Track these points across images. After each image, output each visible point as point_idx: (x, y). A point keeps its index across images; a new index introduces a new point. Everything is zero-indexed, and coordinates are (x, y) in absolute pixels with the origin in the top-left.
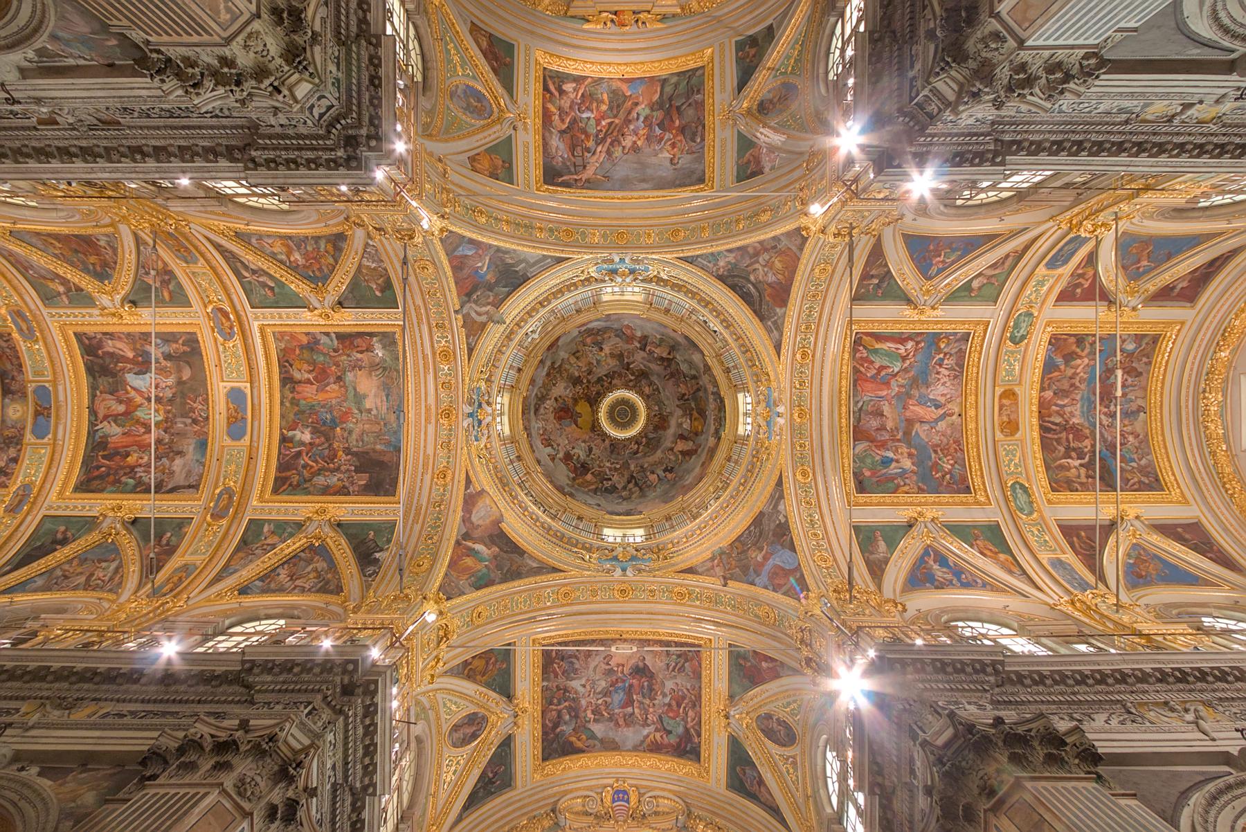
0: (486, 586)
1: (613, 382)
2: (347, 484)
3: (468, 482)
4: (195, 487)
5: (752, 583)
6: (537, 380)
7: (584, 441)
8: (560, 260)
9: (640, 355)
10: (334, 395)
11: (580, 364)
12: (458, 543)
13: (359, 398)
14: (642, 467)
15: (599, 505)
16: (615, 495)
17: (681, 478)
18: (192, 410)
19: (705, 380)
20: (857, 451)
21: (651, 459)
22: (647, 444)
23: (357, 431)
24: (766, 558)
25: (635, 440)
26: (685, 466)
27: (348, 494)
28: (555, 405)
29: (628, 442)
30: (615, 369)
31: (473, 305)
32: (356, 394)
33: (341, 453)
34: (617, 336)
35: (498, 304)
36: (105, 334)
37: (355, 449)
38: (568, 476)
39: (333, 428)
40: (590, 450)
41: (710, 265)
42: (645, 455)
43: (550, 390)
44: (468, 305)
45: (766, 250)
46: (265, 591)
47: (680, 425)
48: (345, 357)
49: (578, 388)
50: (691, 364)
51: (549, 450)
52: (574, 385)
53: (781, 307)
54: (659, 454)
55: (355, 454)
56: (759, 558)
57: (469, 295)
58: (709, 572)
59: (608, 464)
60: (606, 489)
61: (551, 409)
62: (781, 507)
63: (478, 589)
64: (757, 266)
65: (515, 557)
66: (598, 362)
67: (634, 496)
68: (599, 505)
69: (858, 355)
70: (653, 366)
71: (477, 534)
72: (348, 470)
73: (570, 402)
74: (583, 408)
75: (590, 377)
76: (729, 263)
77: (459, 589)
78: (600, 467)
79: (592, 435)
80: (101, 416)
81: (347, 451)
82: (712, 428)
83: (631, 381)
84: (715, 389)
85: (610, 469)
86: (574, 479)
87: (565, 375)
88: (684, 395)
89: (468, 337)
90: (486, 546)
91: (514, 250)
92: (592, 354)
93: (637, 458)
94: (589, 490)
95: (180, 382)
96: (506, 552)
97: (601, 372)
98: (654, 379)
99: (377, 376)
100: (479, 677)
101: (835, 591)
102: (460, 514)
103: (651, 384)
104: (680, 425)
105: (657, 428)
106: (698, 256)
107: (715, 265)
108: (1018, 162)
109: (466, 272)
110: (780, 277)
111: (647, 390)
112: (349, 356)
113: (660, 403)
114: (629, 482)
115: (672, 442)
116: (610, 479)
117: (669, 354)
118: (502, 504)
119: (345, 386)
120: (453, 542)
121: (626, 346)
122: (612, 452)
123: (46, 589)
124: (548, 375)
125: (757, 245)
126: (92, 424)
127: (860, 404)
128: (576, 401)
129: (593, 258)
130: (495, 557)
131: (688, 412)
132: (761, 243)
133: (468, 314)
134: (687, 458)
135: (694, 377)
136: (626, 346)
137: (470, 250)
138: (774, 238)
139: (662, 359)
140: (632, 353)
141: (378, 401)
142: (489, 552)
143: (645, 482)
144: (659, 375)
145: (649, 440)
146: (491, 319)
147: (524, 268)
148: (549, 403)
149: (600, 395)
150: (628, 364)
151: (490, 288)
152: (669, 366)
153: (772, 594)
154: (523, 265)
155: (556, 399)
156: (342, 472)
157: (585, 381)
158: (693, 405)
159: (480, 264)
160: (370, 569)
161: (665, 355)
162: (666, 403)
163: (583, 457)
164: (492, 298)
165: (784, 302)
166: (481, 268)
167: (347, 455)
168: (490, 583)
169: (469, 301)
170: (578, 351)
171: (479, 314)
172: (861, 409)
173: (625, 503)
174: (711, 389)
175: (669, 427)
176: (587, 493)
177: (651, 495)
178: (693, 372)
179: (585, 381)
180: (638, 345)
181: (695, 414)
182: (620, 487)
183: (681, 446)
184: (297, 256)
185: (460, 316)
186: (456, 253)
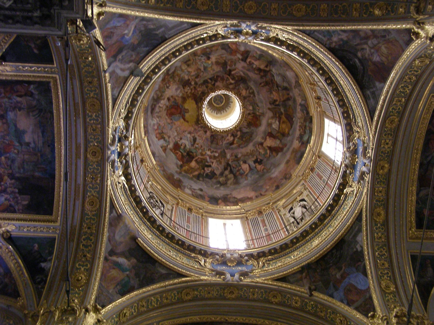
1: (217, 84)
2: (13, 203)
5: (331, 296)
7: (190, 133)
8: (196, 25)
9: (240, 65)
11: (190, 70)
12: (106, 259)
13: (19, 134)
14: (236, 157)
15: (201, 190)
16: (214, 180)
17: (268, 171)
19: (295, 92)
20: (421, 194)
21: (244, 151)
22: (241, 138)
24: (343, 277)
25: (232, 132)
26: (272, 160)
27: (14, 212)
28: (167, 104)
29: (226, 134)
30: (219, 74)
32: (17, 130)
33: (6, 178)
34: (223, 49)
37: (17, 175)
38: (177, 164)
40: (195, 140)
41: (325, 39)
42: (239, 146)
43: (164, 92)
44: (114, 65)
45: (375, 37)
47: (270, 125)
48: (6, 100)
49: (187, 89)
50: (284, 78)
51: (162, 142)
52: (184, 86)
53: (380, 82)
54: (250, 147)
55: (17, 179)
56: (338, 276)
57: (115, 57)
58: (297, 282)
59: (209, 153)
60: (207, 175)
62: (359, 238)
63: (123, 294)
64: (365, 46)
66: (205, 68)
67: (229, 182)
68: (201, 190)
70: (251, 74)
72: (13, 192)
73: (180, 101)
74: (190, 105)
75: (197, 80)
76: (342, 40)
78: (202, 155)
79: (197, 128)
81: (11, 176)
82: (298, 133)
83: (231, 84)
84: (303, 102)
85: (210, 157)
86: (181, 166)
87: (177, 79)
88: (275, 101)
89: (113, 89)
90: (126, 258)
91: (157, 19)
92: (202, 62)
93: (232, 149)
94: (193, 176)
97: (208, 75)
98: (251, 84)
99: (34, 116)
101: (396, 316)
103: (247, 88)
104: (270, 125)
105: (250, 124)
106: (315, 31)
107: (328, 39)
109: (115, 38)
110: (384, 59)
111: (244, 93)
112: (10, 98)
113: (254, 104)
114: (225, 169)
115: (263, 138)
116: (210, 166)
117: (266, 66)
118: (136, 219)
119: (7, 123)
121: (230, 57)
122: (212, 142)
125: (370, 32)
127: (429, 159)
128: (184, 99)
129: (223, 24)
130: (134, 267)
131: (277, 115)
132: (372, 31)
134: (274, 153)
135: (286, 89)
136: (230, 57)
137: (119, 22)
138: (385, 30)
139: (259, 70)
140: (234, 62)
141: (36, 137)
142: (129, 263)
143: (238, 170)
144: (255, 82)
145: (243, 134)
146: (132, 73)
148: (163, 103)
149: (204, 95)
150: (230, 71)
152: (265, 76)
153: (347, 308)
154: (163, 29)
155: (169, 99)
156: (7, 193)
157: (193, 83)
158: (282, 110)
159: (126, 32)
160: (39, 278)
161: (262, 67)
162: (260, 105)
163: (188, 146)
164: (134, 56)
165: (384, 79)
166: (127, 34)
167: (11, 179)
168: (132, 290)
169: (115, 60)
170: (189, 60)
171: (123, 70)
172: (429, 162)
173: (222, 188)
174: (299, 100)
175: (260, 125)
176: (191, 179)
177: (243, 182)
178: (285, 84)
179: (193, 83)
180: (240, 57)
181: (284, 118)
182: (218, 172)
183: (269, 142)
186: (108, 26)
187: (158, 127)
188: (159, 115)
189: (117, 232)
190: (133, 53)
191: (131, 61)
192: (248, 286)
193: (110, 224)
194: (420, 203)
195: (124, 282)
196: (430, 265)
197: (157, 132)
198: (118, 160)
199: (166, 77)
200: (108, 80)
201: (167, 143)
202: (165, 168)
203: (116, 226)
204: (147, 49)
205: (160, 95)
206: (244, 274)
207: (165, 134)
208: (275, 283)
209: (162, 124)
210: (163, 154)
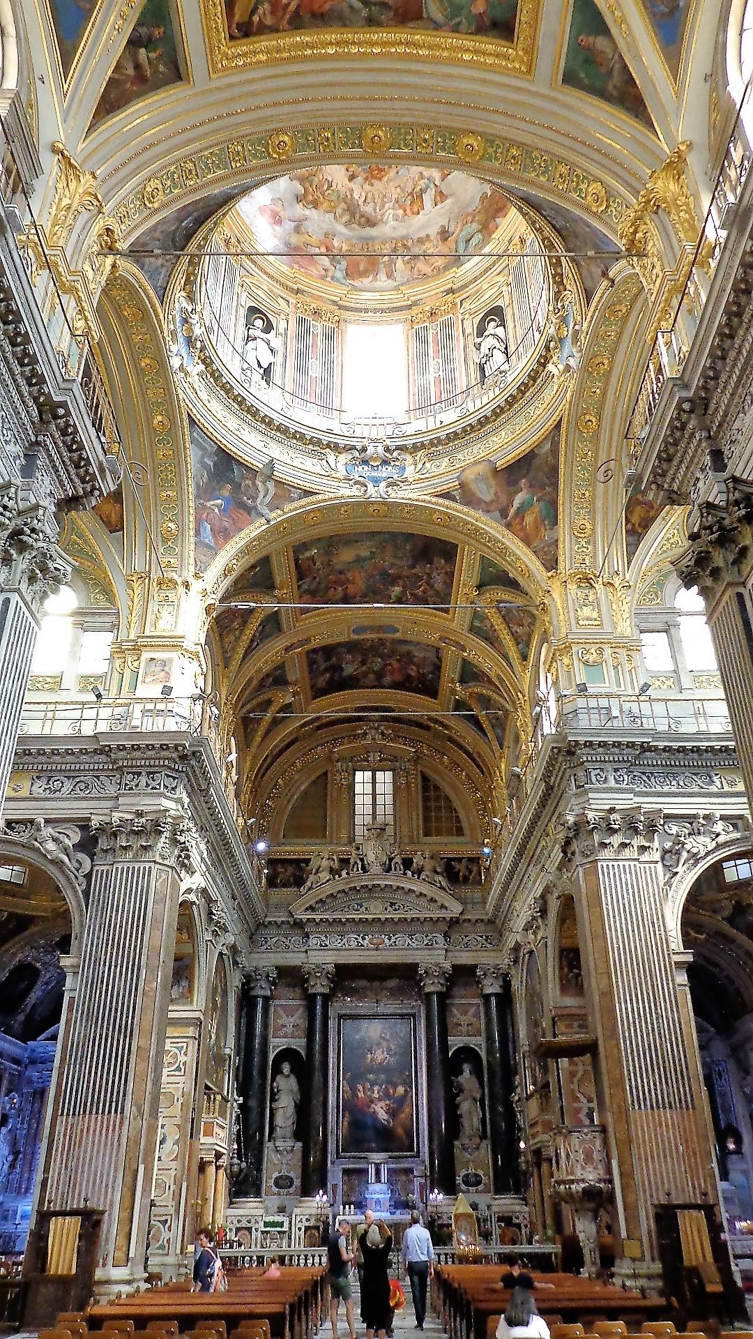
0: (556, 510)
3: (447, 495)
4: (438, 650)
6: (325, 227)
10: (357, 574)
13: (359, 560)
18: (372, 646)
20: (439, 16)
23: (393, 560)
28: (360, 179)
31: (258, 501)
35: (253, 472)
36: (312, 687)
39: (389, 575)
41: (163, 271)
46: (528, 645)
51: (428, 198)
57: (249, 510)
61: (367, 187)
65: (537, 462)
69: (269, 21)
71: (503, 500)
72: (430, 568)
77: (551, 544)
80: (376, 684)
95: (349, 652)
96: (528, 471)
100: (652, 514)
102: (478, 514)
106: (155, 288)
108: (24, 300)
120: (506, 532)
123: (504, 730)
124: (315, 205)
126: (385, 687)
133: (267, 505)
142: (525, 491)
146: (270, 477)
147: (209, 457)
148: (358, 191)
151: (237, 487)
155: (352, 178)
159: (216, 510)
168: (554, 504)
169: (255, 508)
184: (235, 625)
185: (273, 515)
187: (400, 207)
188: (379, 202)
189: (480, 496)
190: (243, 484)
191: (254, 483)
192: (590, 346)
193: (468, 504)
194: (458, 20)
195: (544, 512)
196: (591, 39)
197: (408, 211)
198: (392, 464)
199: (311, 198)
200: (279, 512)
201: (432, 185)
202: (470, 210)
203: (474, 495)
204: (235, 467)
205: (343, 205)
206: (576, 333)
207: (415, 186)
208: (592, 309)
209: (395, 193)
210: (449, 201)
